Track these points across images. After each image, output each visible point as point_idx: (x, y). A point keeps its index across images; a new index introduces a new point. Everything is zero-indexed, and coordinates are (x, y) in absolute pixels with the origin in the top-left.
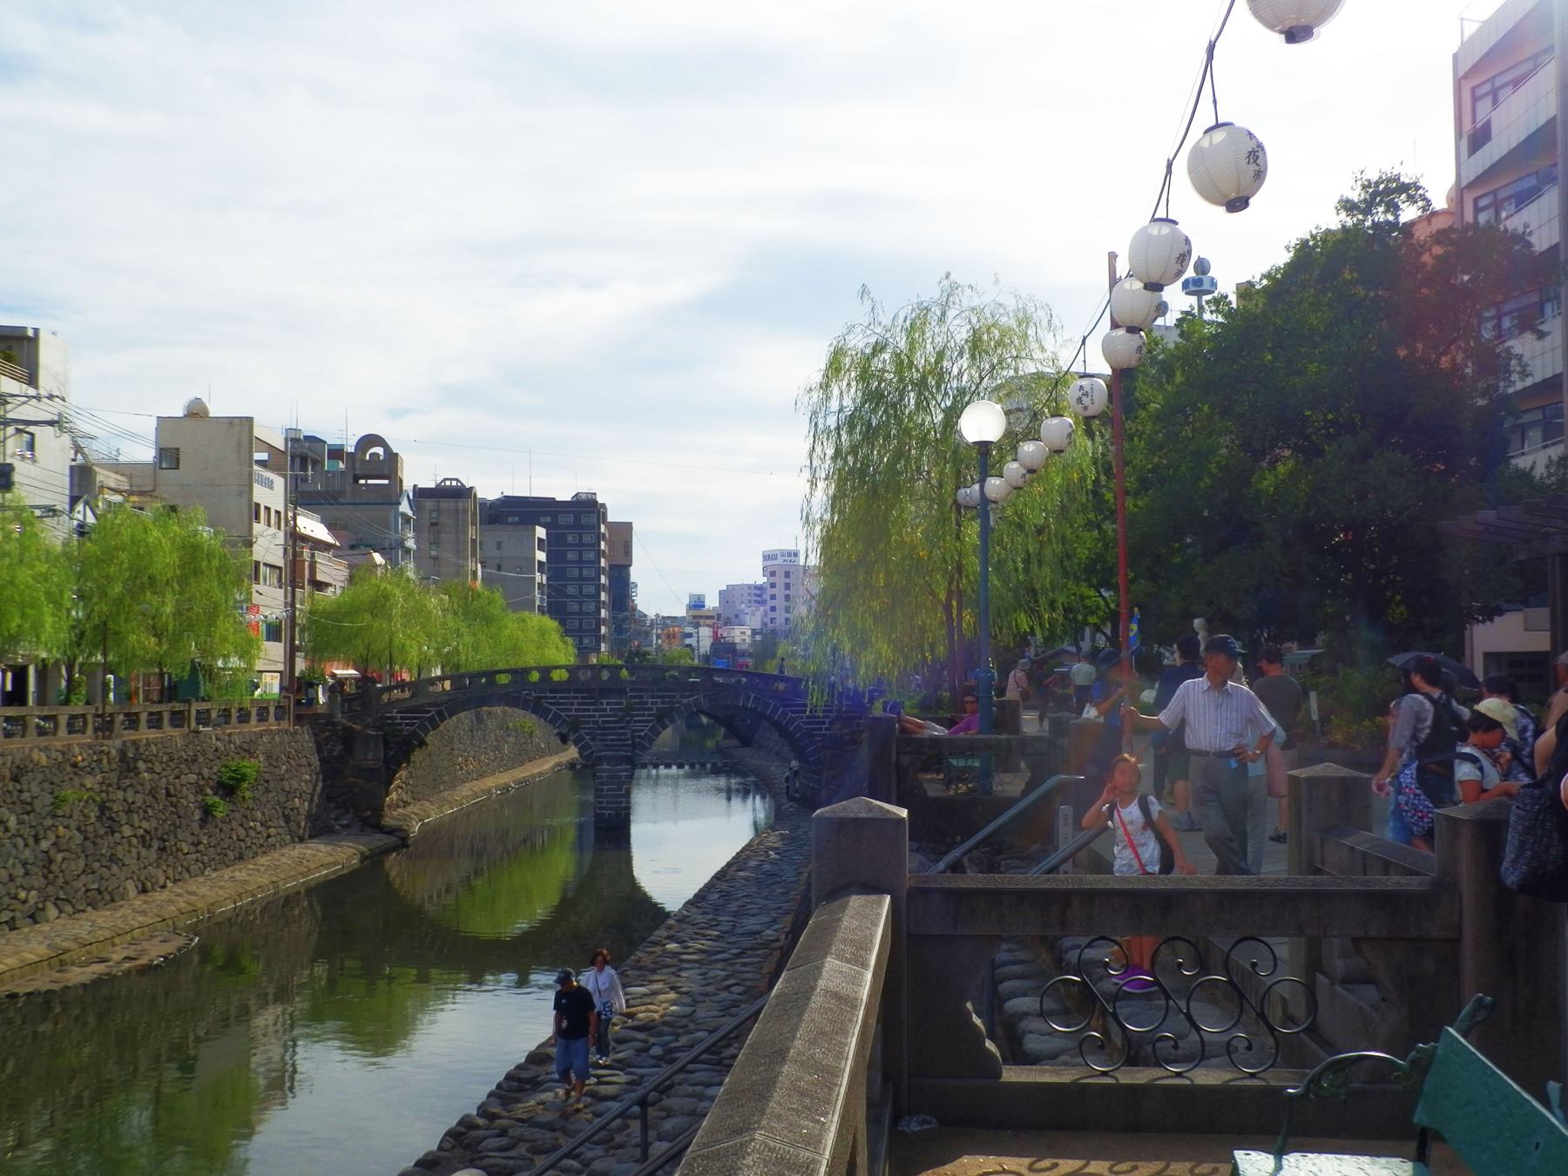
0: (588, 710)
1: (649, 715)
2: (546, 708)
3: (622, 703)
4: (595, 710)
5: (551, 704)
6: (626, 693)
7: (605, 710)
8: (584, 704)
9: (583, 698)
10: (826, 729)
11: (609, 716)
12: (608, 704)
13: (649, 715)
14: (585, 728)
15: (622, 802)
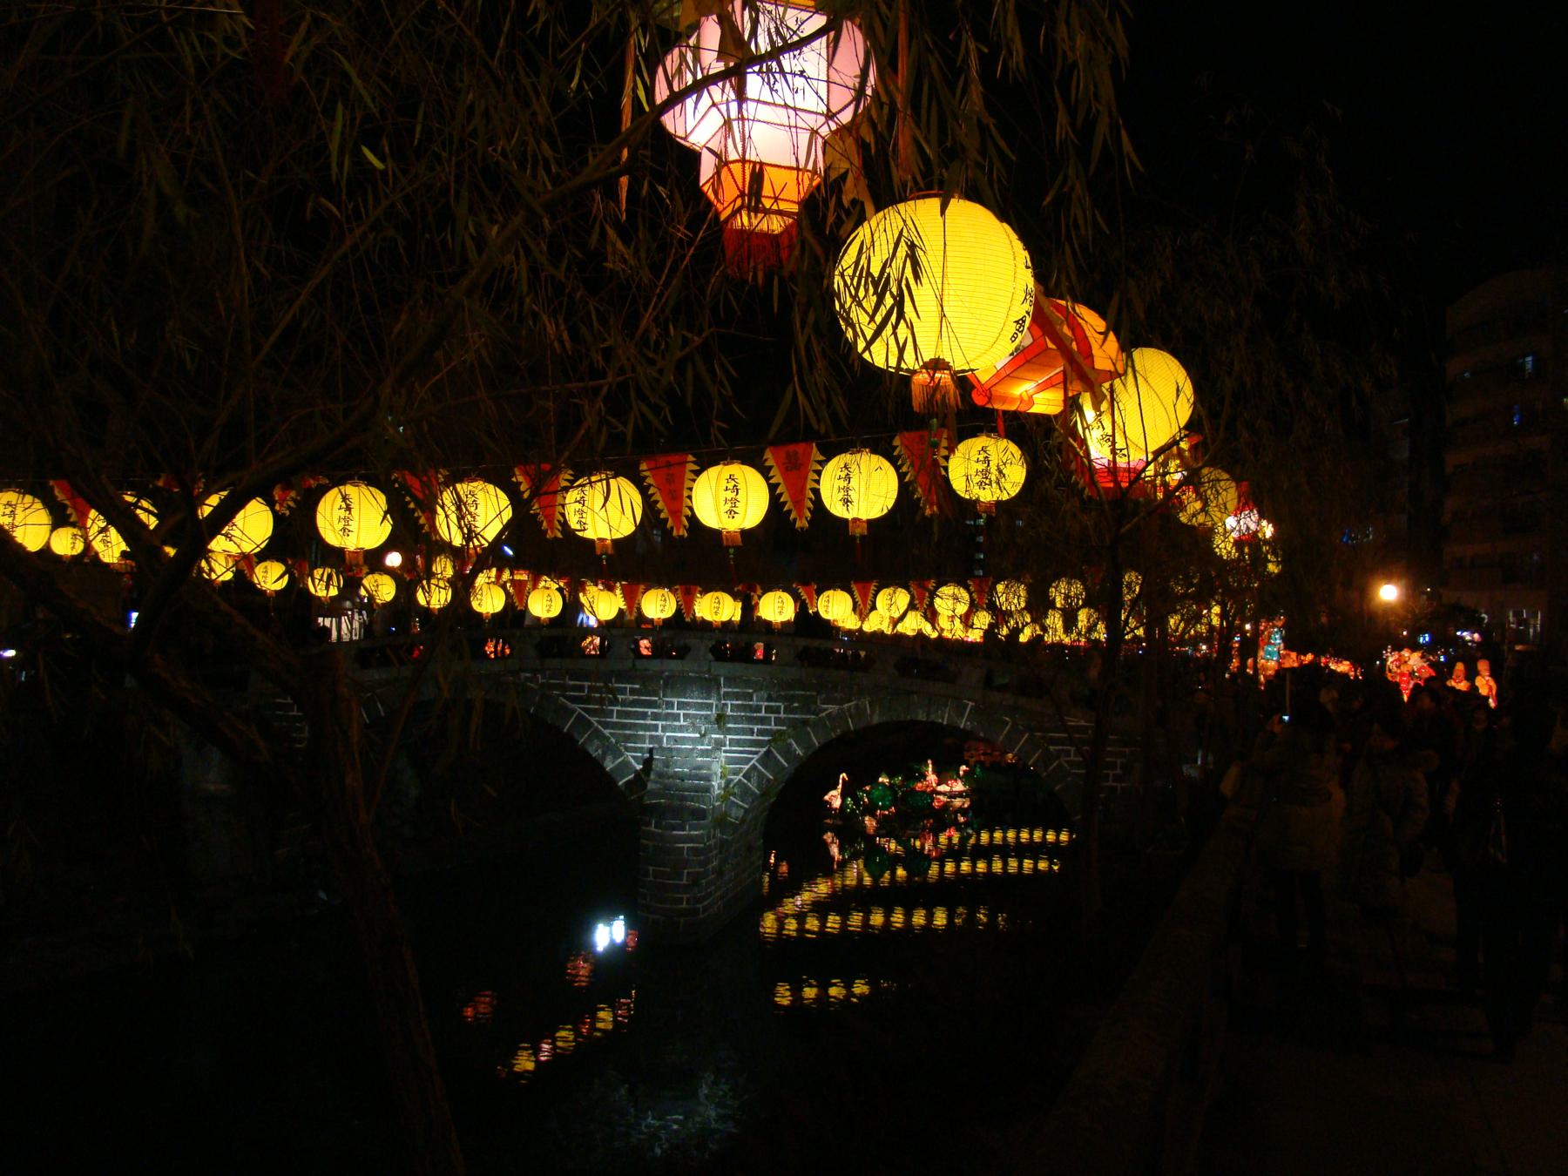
0: (644, 716)
1: (761, 733)
2: (564, 707)
3: (709, 707)
4: (656, 717)
5: (574, 700)
6: (719, 685)
7: (676, 717)
8: (634, 703)
9: (633, 692)
10: (1117, 779)
11: (681, 729)
12: (681, 706)
13: (761, 733)
14: (635, 750)
15: (680, 901)
